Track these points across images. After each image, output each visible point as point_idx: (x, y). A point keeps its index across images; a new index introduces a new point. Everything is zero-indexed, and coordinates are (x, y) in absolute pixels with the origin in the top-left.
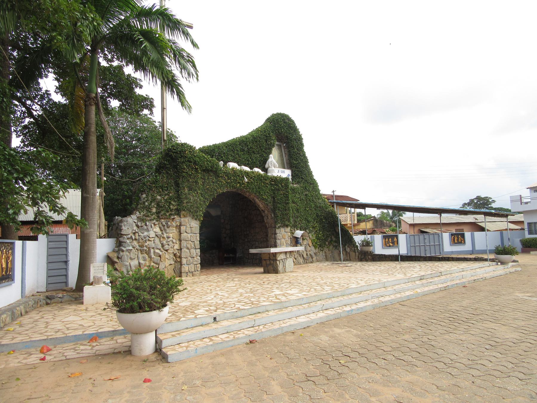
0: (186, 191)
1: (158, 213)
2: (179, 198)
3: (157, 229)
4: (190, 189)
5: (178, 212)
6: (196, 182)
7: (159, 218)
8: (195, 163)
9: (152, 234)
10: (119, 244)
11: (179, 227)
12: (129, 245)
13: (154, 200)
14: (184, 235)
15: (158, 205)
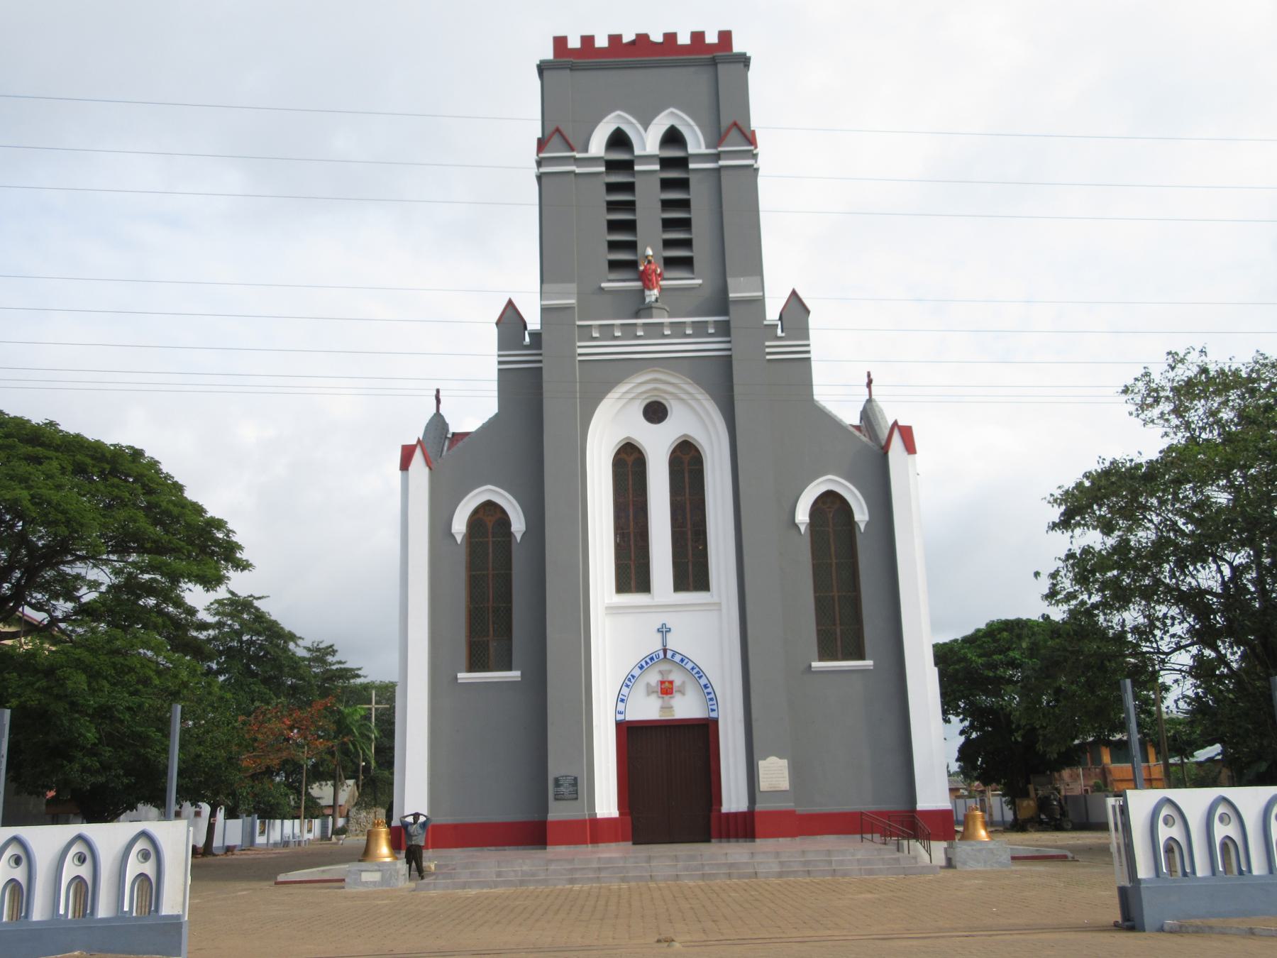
0: (379, 795)
1: (365, 806)
2: (375, 799)
3: (365, 814)
4: (381, 794)
5: (375, 806)
6: (385, 791)
7: (365, 809)
8: (384, 781)
9: (362, 816)
10: (348, 821)
11: (375, 813)
12: (352, 821)
13: (364, 800)
14: (377, 816)
15: (366, 803)
